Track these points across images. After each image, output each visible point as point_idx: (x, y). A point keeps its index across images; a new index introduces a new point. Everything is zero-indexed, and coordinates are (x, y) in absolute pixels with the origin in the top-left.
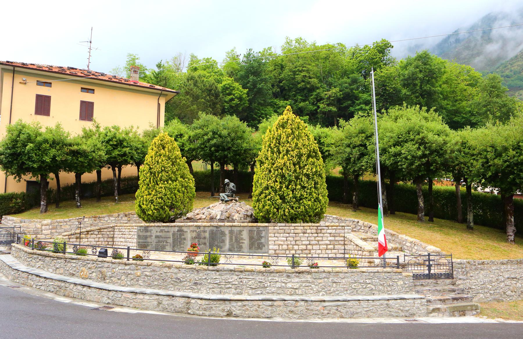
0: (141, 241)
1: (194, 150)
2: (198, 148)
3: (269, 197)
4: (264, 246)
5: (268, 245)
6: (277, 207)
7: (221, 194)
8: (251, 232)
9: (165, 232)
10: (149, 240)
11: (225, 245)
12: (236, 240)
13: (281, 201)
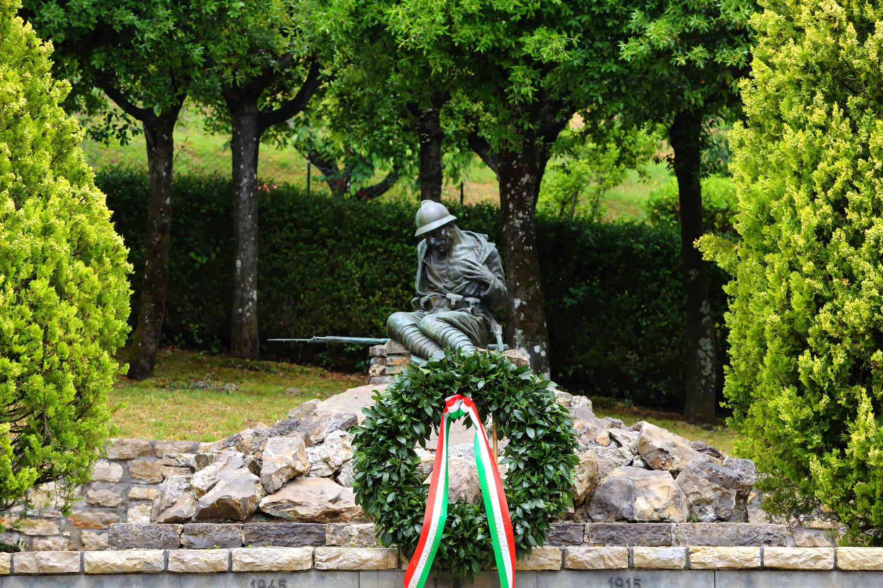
7: (400, 319)
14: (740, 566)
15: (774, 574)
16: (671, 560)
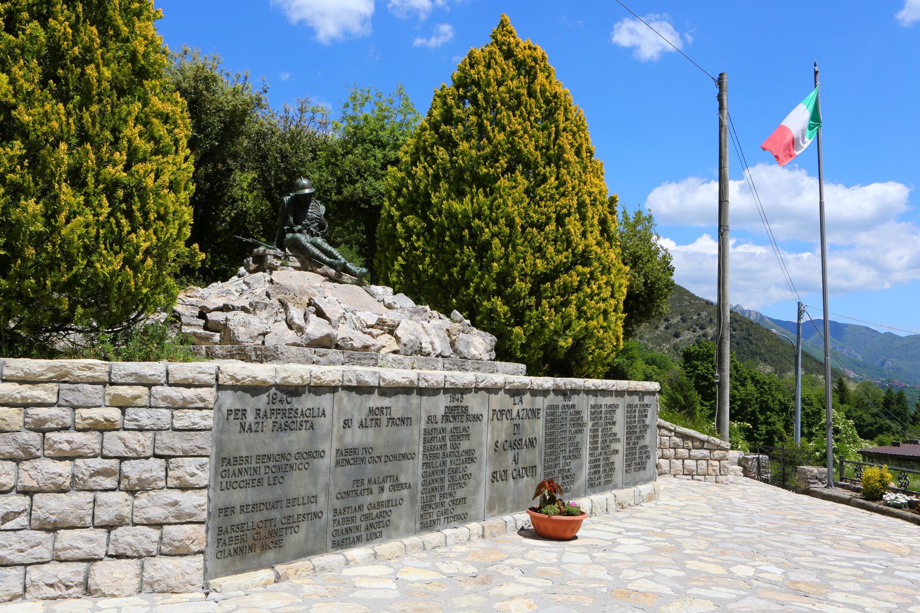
0: (239, 497)
10: (298, 483)
11: (580, 467)
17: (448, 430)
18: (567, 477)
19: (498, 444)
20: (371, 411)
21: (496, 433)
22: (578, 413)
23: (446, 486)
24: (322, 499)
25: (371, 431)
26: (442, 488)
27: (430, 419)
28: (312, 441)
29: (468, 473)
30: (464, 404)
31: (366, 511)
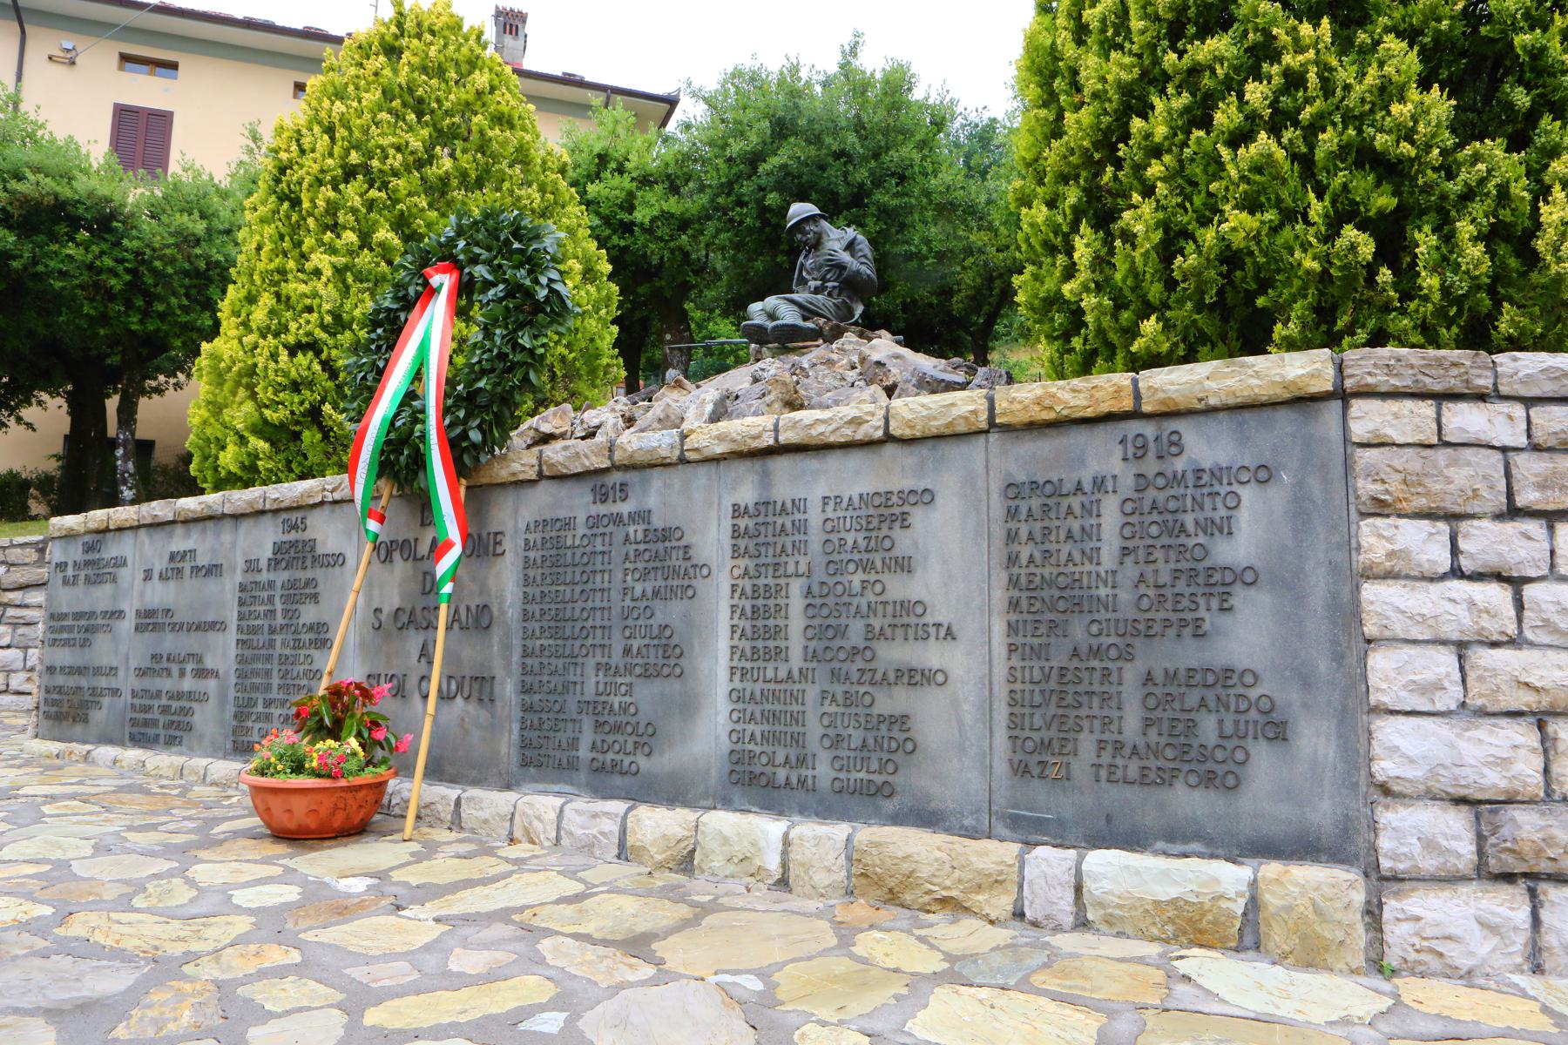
1: (684, 224)
2: (705, 217)
3: (1256, 93)
4: (1278, 731)
5: (1356, 711)
6: (1385, 201)
8: (1036, 509)
9: (196, 570)
11: (688, 707)
12: (825, 631)
13: (1439, 104)
14: (745, 448)
15: (799, 457)
16: (655, 449)
17: (279, 584)
18: (617, 728)
19: (383, 617)
20: (172, 557)
21: (376, 592)
22: (666, 534)
23: (275, 687)
24: (121, 673)
25: (172, 584)
26: (268, 688)
27: (251, 566)
28: (114, 598)
29: (314, 667)
30: (307, 535)
31: (164, 701)
